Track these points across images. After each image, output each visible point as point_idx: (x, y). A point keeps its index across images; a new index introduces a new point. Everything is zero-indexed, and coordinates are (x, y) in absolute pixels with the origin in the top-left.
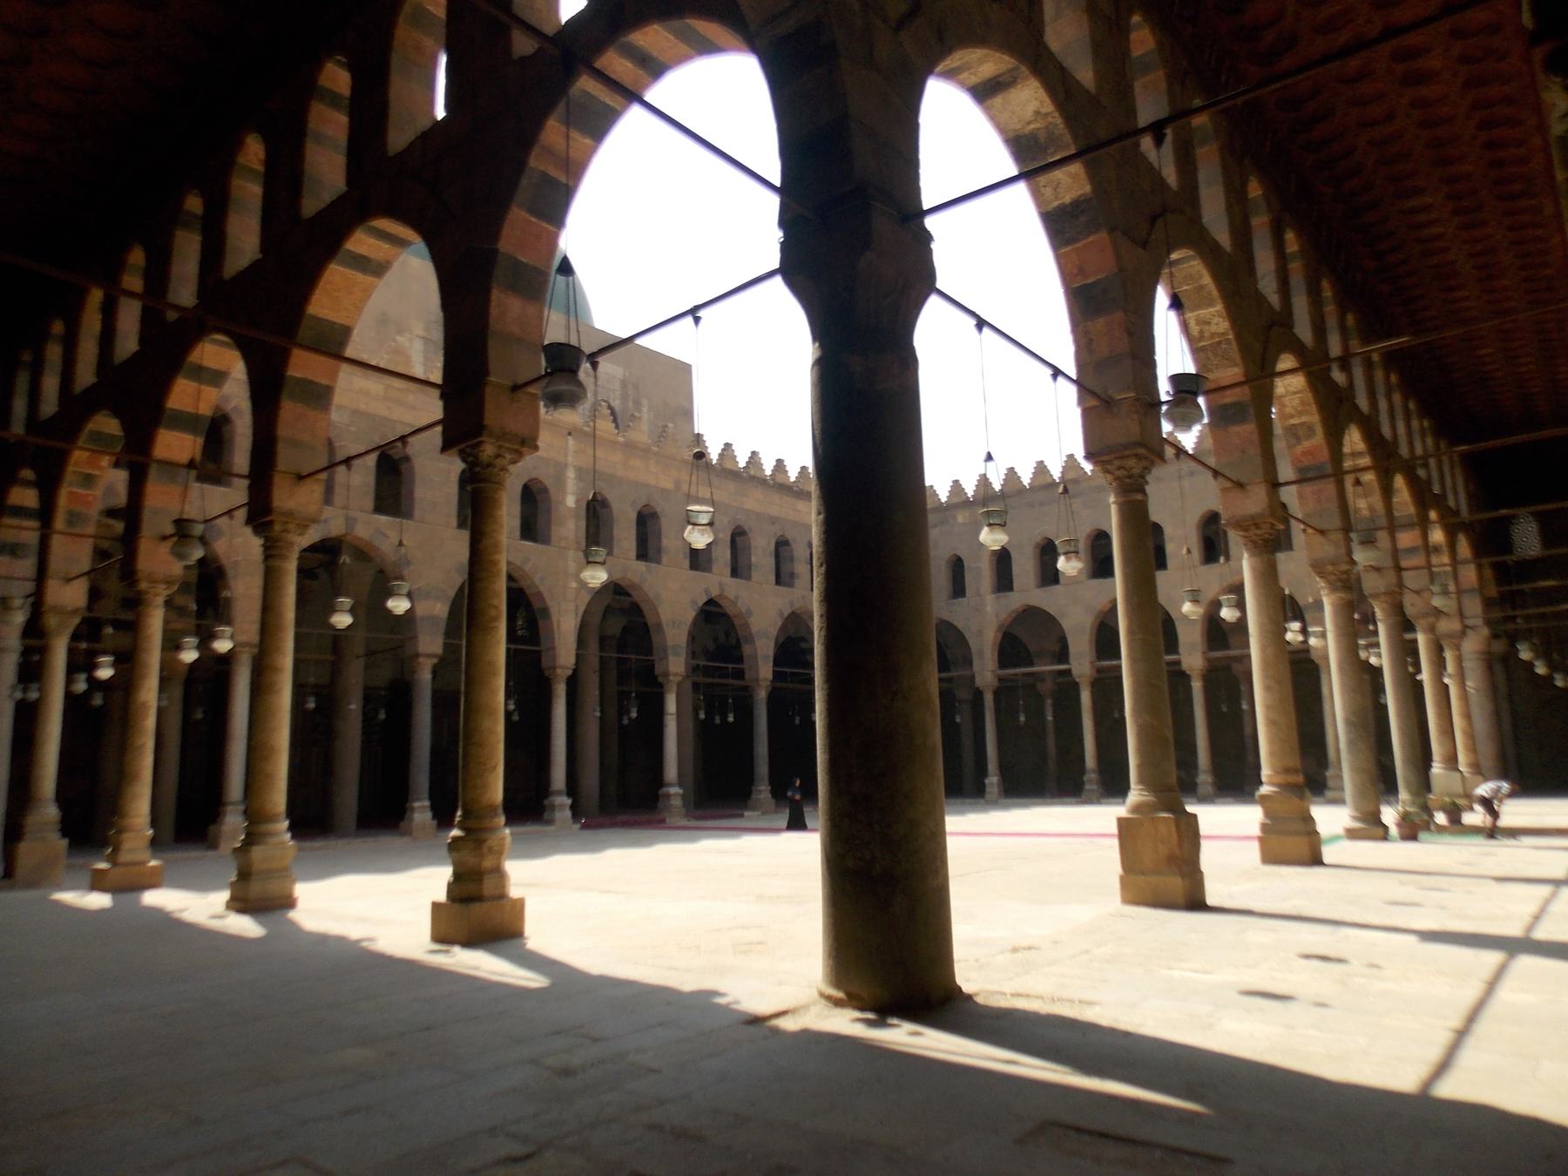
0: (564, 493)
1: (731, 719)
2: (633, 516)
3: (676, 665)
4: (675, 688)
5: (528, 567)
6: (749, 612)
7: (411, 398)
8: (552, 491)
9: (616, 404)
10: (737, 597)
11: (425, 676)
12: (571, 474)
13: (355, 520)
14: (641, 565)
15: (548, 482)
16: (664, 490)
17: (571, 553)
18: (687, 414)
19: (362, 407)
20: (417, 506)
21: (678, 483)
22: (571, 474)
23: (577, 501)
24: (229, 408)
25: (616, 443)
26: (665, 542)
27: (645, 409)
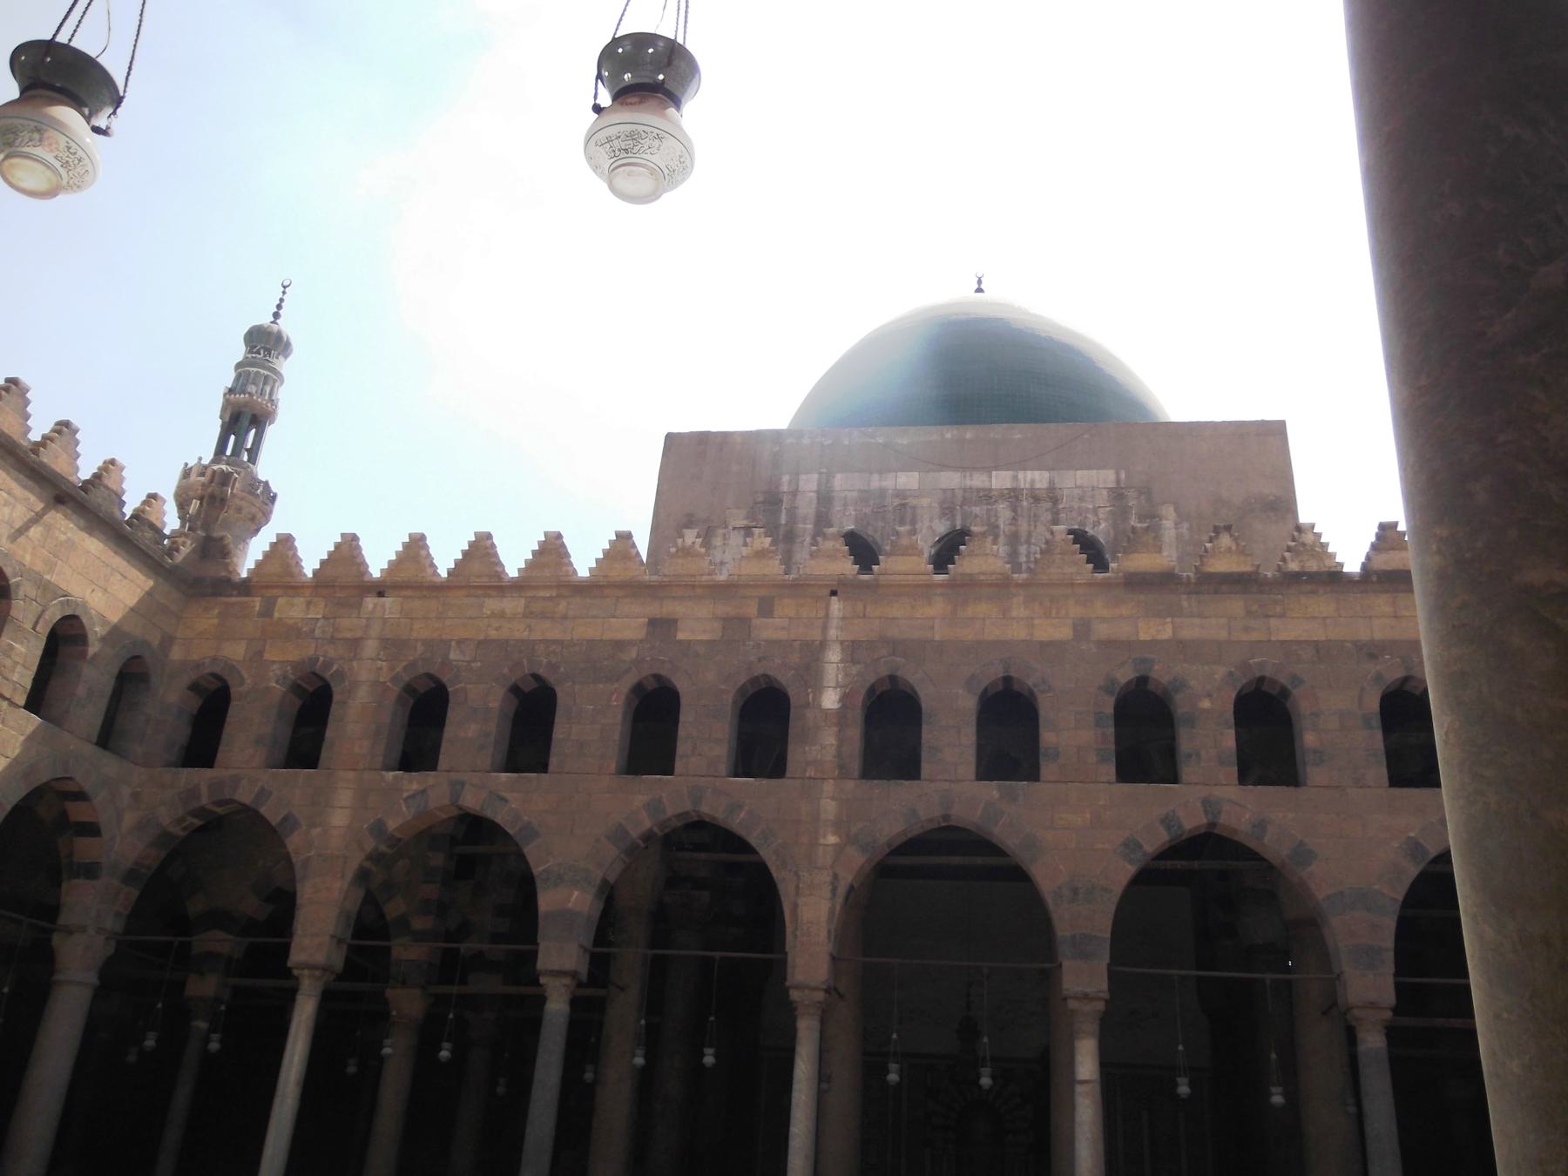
0: (819, 689)
1: (709, 1060)
2: (969, 703)
3: (1084, 979)
4: (1092, 1026)
5: (736, 824)
6: (1303, 855)
7: (563, 604)
8: (791, 692)
9: (1100, 531)
10: (1261, 825)
11: (557, 1006)
12: (834, 656)
13: (463, 784)
14: (992, 790)
15: (785, 679)
16: (1044, 645)
17: (829, 787)
18: (1282, 503)
19: (493, 634)
20: (554, 749)
21: (1082, 629)
22: (834, 656)
23: (844, 699)
24: (327, 675)
25: (929, 586)
26: (1047, 737)
27: (1168, 523)
